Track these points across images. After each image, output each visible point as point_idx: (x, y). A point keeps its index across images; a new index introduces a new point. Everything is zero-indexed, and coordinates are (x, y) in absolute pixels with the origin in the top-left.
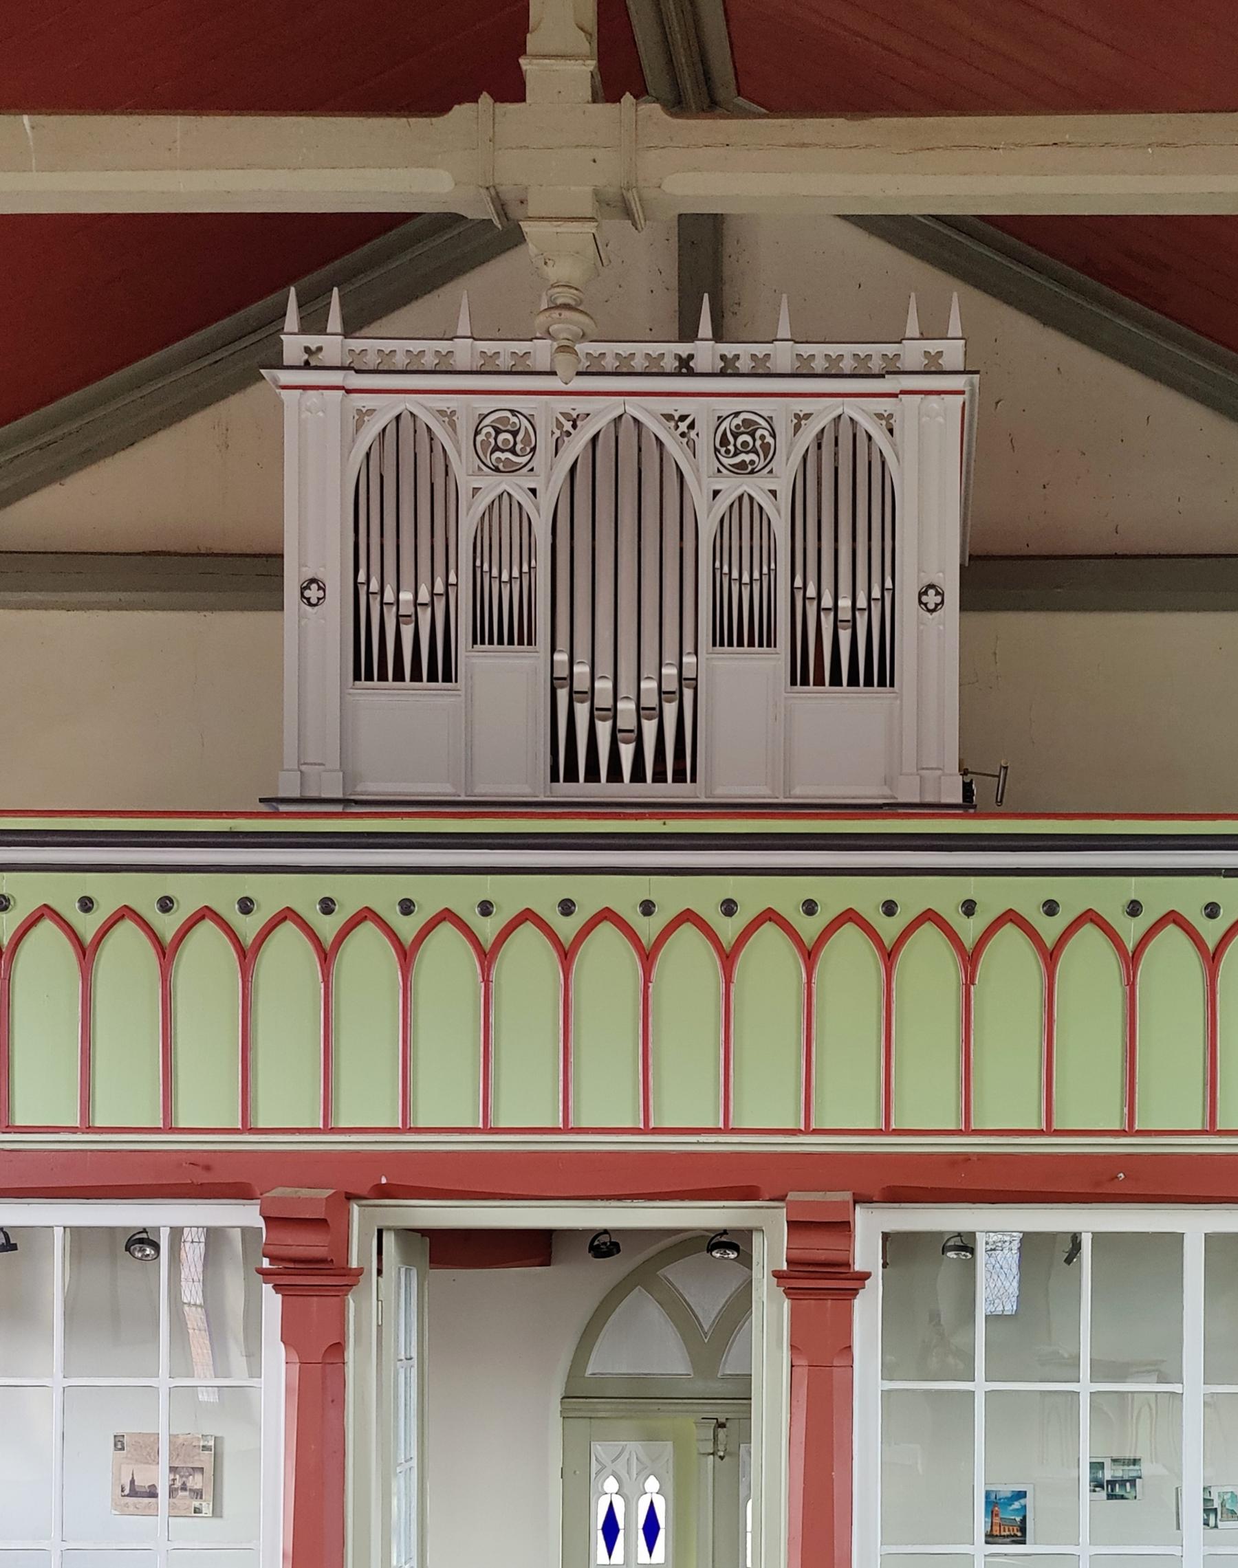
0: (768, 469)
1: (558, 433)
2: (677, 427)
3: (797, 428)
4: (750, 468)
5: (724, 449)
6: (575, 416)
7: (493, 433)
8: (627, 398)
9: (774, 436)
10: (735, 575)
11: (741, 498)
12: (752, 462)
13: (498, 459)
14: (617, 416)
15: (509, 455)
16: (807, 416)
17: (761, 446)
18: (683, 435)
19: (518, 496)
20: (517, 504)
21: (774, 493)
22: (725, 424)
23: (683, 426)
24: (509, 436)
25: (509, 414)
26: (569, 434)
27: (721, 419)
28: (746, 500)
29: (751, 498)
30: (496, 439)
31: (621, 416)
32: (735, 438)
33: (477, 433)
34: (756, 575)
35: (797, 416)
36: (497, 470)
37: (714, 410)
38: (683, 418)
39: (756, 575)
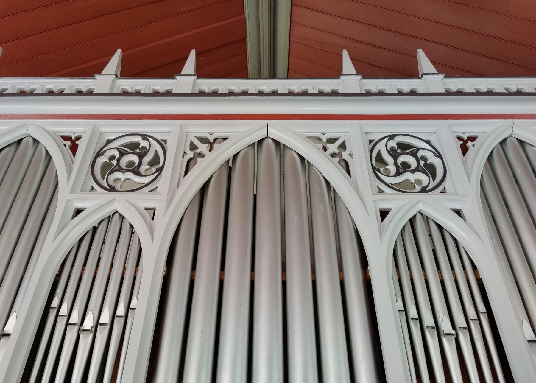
0: (440, 188)
1: (190, 154)
2: (325, 149)
3: (464, 150)
4: (418, 188)
5: (383, 168)
6: (211, 140)
7: (117, 154)
8: (270, 121)
9: (440, 156)
10: (428, 321)
11: (412, 221)
12: (418, 181)
13: (118, 179)
14: (257, 140)
15: (130, 175)
16: (473, 139)
17: (424, 165)
18: (333, 155)
19: (132, 217)
20: (128, 226)
21: (458, 212)
22: (381, 147)
23: (333, 148)
24: (135, 158)
25: (138, 139)
26: (201, 155)
27: (373, 144)
28: (420, 224)
29: (426, 219)
30: (118, 161)
31: (260, 142)
32: (395, 157)
33: (99, 154)
34: (460, 321)
35: (460, 138)
36: (112, 189)
37: (366, 133)
38: (332, 141)
39: (460, 321)
